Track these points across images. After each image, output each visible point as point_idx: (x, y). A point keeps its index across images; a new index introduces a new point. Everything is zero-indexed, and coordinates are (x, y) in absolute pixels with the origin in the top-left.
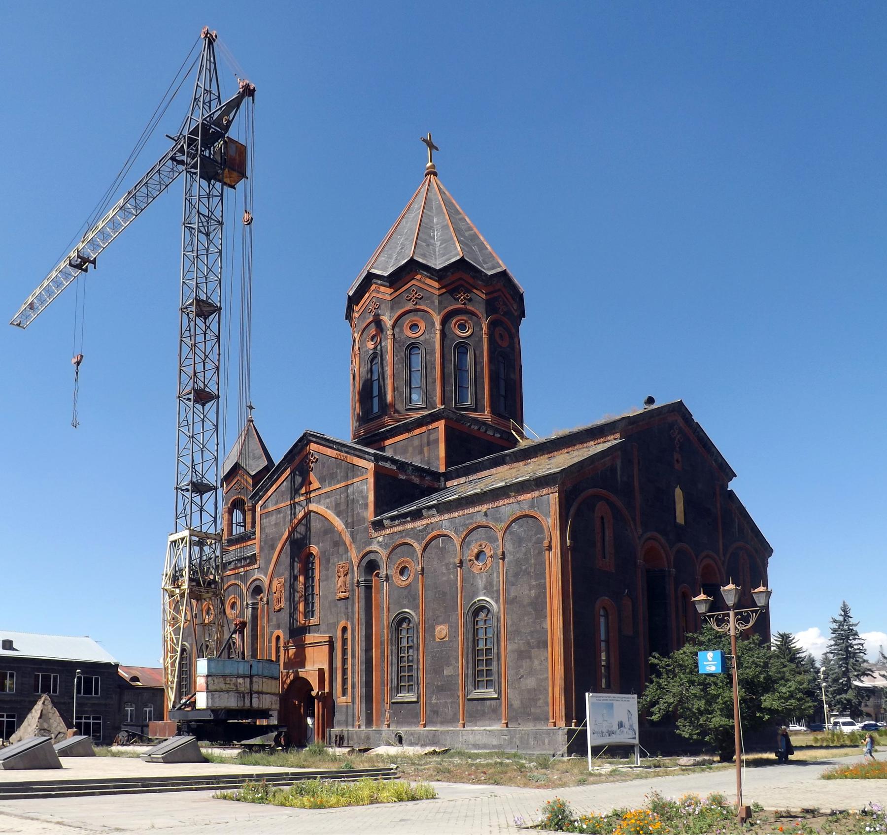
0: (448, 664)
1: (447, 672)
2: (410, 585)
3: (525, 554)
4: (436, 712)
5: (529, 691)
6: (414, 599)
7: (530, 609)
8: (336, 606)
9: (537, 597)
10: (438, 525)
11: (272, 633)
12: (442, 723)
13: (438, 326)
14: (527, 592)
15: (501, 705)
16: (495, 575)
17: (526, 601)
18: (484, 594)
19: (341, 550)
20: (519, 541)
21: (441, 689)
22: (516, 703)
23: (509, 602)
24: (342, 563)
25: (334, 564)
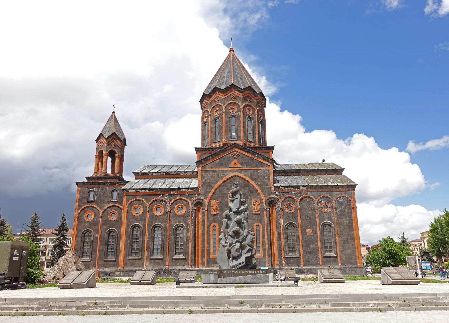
0: (313, 244)
2: (293, 212)
3: (344, 208)
4: (309, 261)
5: (349, 254)
6: (296, 218)
7: (347, 227)
8: (252, 216)
9: (349, 223)
11: (210, 225)
12: (311, 265)
15: (337, 259)
17: (345, 224)
18: (328, 220)
19: (254, 194)
21: (310, 253)
22: (344, 258)
24: (256, 200)
25: (251, 199)
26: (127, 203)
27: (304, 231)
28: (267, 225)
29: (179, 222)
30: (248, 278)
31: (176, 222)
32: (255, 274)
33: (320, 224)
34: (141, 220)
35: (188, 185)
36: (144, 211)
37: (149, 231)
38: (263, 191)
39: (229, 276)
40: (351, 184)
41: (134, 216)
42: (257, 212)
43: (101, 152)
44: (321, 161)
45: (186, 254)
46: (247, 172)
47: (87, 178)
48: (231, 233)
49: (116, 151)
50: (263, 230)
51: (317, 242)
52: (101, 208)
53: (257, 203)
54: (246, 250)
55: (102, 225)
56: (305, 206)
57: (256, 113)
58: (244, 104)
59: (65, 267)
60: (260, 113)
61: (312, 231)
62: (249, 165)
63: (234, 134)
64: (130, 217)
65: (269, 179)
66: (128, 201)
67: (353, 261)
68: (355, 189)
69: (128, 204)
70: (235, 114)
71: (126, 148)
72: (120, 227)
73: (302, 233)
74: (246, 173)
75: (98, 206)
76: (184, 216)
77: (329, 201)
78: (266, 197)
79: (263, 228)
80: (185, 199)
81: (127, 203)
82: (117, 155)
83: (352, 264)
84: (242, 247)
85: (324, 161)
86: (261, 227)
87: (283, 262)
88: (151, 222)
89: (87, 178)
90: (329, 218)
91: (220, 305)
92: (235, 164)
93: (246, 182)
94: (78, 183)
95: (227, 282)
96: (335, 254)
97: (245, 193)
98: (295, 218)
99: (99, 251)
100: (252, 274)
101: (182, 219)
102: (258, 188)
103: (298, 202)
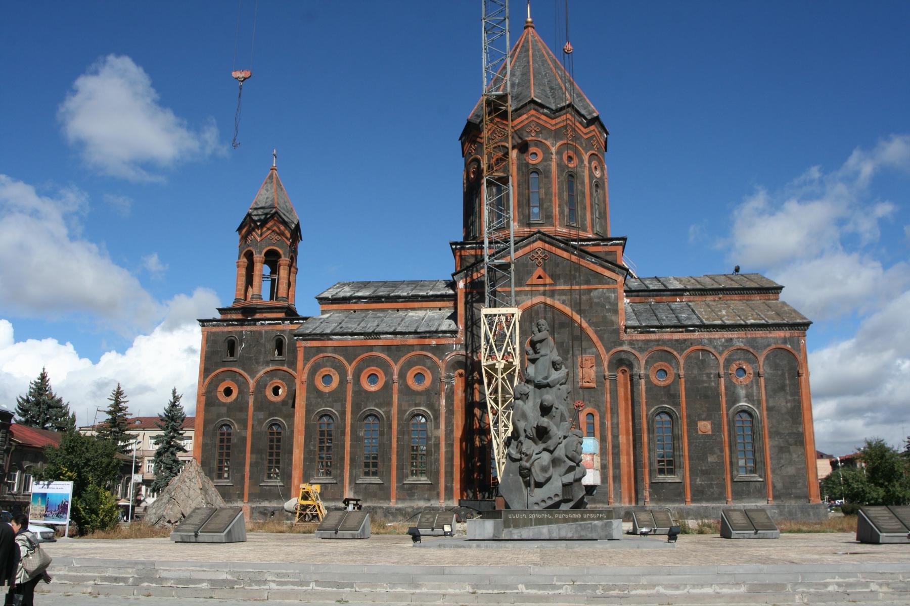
0: (713, 453)
1: (711, 459)
5: (790, 477)
8: (578, 393)
9: (793, 408)
10: (699, 342)
12: (708, 500)
13: (587, 165)
14: (783, 404)
16: (755, 387)
17: (784, 410)
18: (746, 402)
20: (776, 367)
21: (705, 473)
22: (779, 485)
23: (769, 409)
26: (305, 365)
27: (692, 425)
28: (612, 413)
29: (416, 405)
30: (565, 530)
31: (410, 406)
32: (583, 519)
33: (728, 410)
34: (336, 401)
35: (436, 324)
36: (343, 382)
37: (352, 425)
38: (601, 338)
39: (527, 523)
40: (798, 321)
41: (320, 394)
42: (587, 385)
43: (249, 256)
44: (732, 270)
45: (435, 475)
46: (565, 295)
47: (221, 311)
48: (532, 433)
49: (281, 252)
50: (602, 425)
51: (722, 450)
52: (252, 375)
53: (589, 364)
54: (563, 469)
55: (255, 411)
56: (696, 372)
57: (586, 163)
58: (558, 144)
59: (183, 497)
60: (593, 164)
61: (709, 427)
62: (570, 279)
63: (536, 210)
64: (312, 396)
65: (616, 311)
66: (306, 359)
67: (798, 491)
68: (807, 332)
69: (308, 366)
70: (539, 167)
71: (301, 246)
72: (290, 416)
73: (688, 431)
74: (564, 297)
75: (244, 370)
76: (427, 392)
77: (748, 361)
78: (608, 351)
79: (602, 418)
80: (430, 355)
81: (305, 365)
82: (284, 260)
83: (798, 497)
84: (555, 462)
85: (737, 270)
86: (597, 418)
87: (646, 493)
88: (356, 407)
89: (221, 311)
90: (749, 397)
91: (507, 587)
92: (540, 277)
93: (563, 318)
94: (203, 322)
95: (524, 537)
96: (761, 476)
97: (563, 343)
98: (673, 397)
99: (251, 466)
100: (575, 520)
101: (424, 398)
102: (590, 332)
103: (682, 362)
